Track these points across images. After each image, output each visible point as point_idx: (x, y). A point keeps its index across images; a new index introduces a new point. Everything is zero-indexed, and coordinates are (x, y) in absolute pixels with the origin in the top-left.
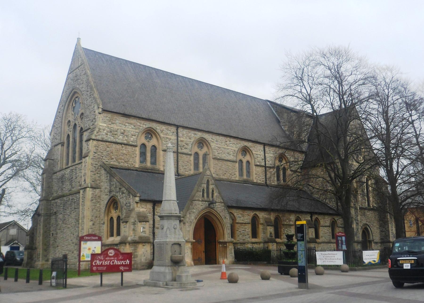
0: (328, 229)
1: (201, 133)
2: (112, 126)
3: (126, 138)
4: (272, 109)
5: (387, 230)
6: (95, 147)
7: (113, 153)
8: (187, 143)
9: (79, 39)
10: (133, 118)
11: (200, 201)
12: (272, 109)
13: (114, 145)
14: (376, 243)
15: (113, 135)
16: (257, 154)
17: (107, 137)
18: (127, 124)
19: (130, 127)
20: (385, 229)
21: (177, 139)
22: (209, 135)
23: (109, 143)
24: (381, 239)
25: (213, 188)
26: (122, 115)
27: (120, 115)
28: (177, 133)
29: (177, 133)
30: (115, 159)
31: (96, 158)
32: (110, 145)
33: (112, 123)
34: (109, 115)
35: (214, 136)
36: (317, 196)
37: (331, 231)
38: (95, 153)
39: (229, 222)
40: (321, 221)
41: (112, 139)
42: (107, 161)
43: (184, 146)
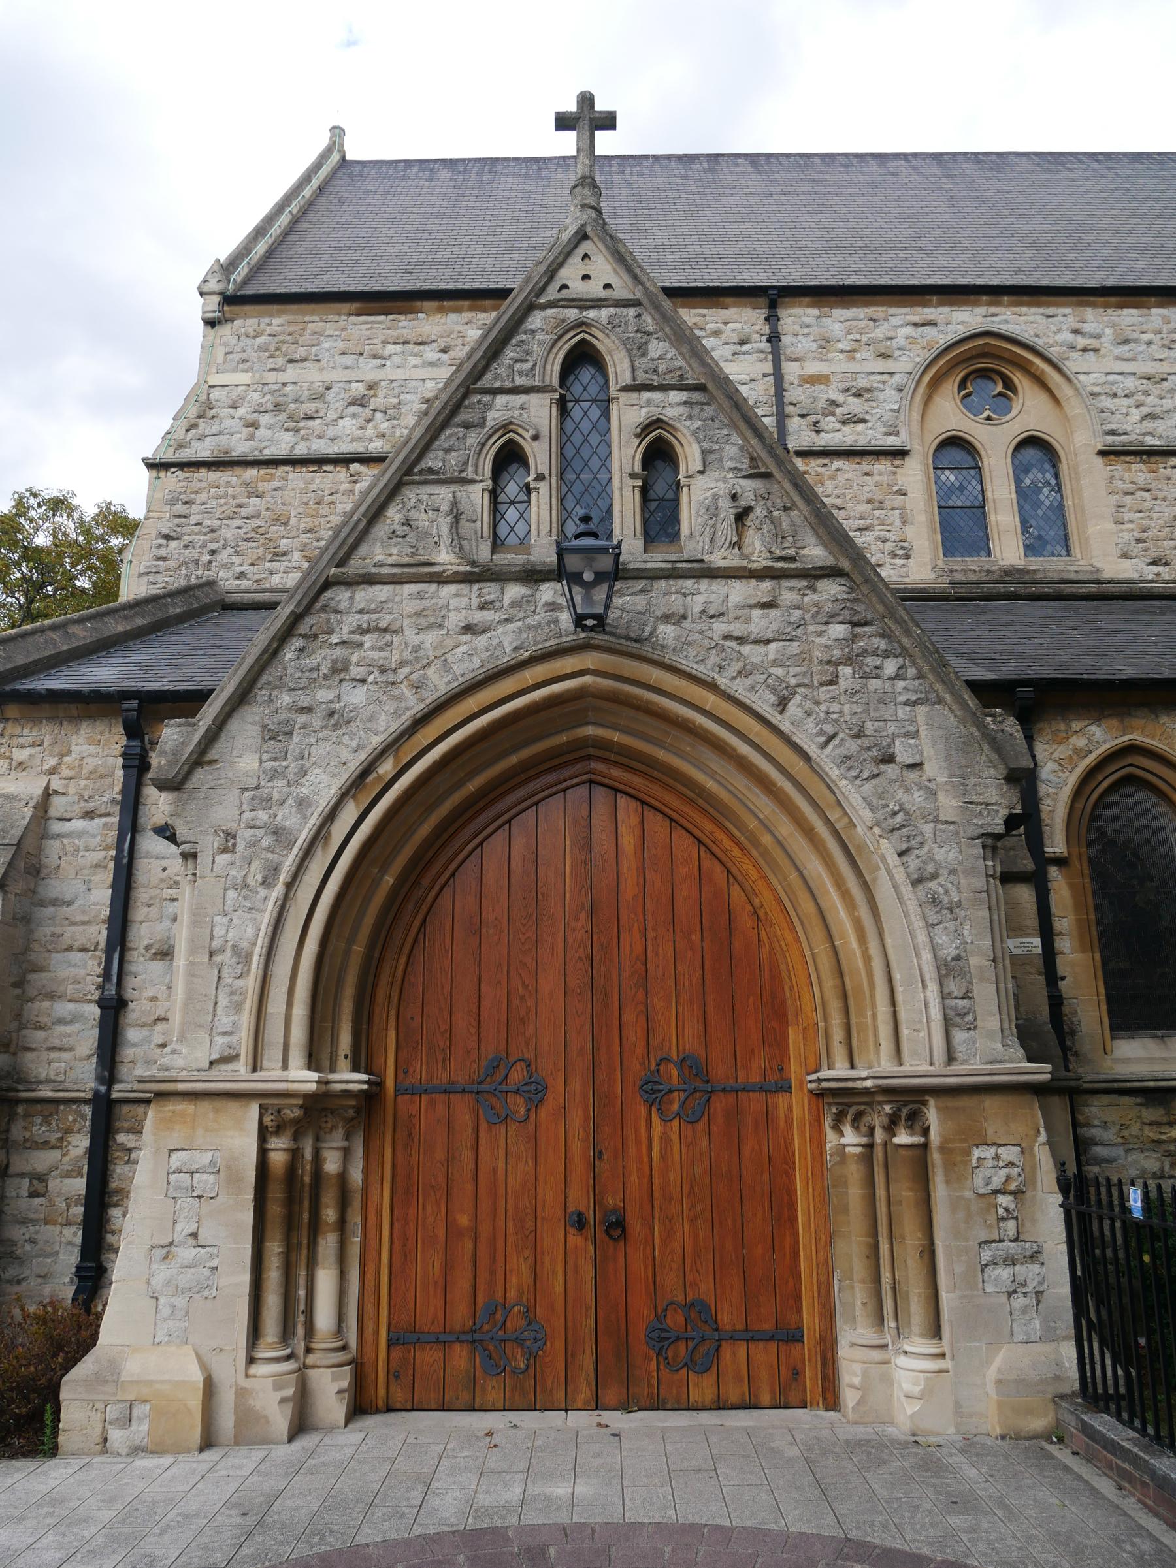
1: (981, 310)
2: (290, 374)
3: (385, 426)
6: (171, 503)
7: (286, 524)
8: (862, 383)
9: (338, 133)
10: (434, 304)
11: (440, 579)
13: (297, 478)
15: (291, 424)
17: (251, 438)
18: (390, 348)
19: (414, 361)
21: (778, 376)
22: (1051, 311)
23: (263, 471)
25: (656, 423)
26: (356, 306)
27: (346, 307)
28: (774, 338)
29: (774, 338)
30: (296, 556)
31: (172, 564)
32: (272, 478)
33: (291, 361)
34: (277, 322)
35: (1089, 313)
38: (167, 537)
39: (949, 804)
41: (282, 444)
42: (242, 575)
43: (833, 403)
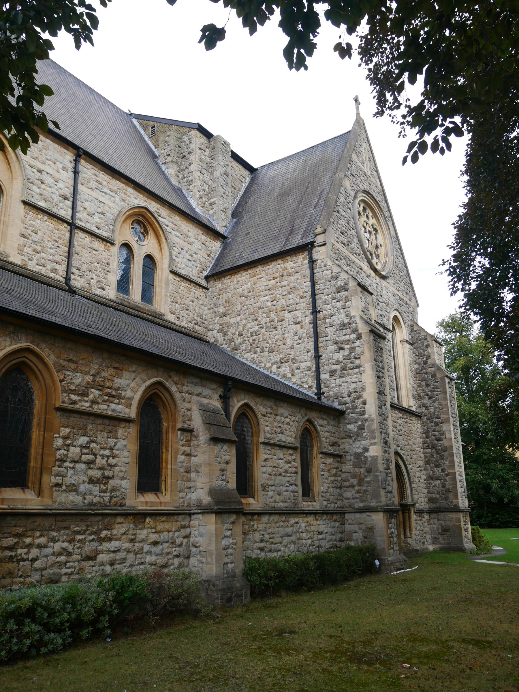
0: (289, 458)
4: (142, 132)
5: (447, 475)
12: (142, 132)
14: (420, 512)
16: (40, 171)
20: (443, 471)
24: (431, 500)
36: (249, 356)
37: (298, 464)
40: (262, 420)
